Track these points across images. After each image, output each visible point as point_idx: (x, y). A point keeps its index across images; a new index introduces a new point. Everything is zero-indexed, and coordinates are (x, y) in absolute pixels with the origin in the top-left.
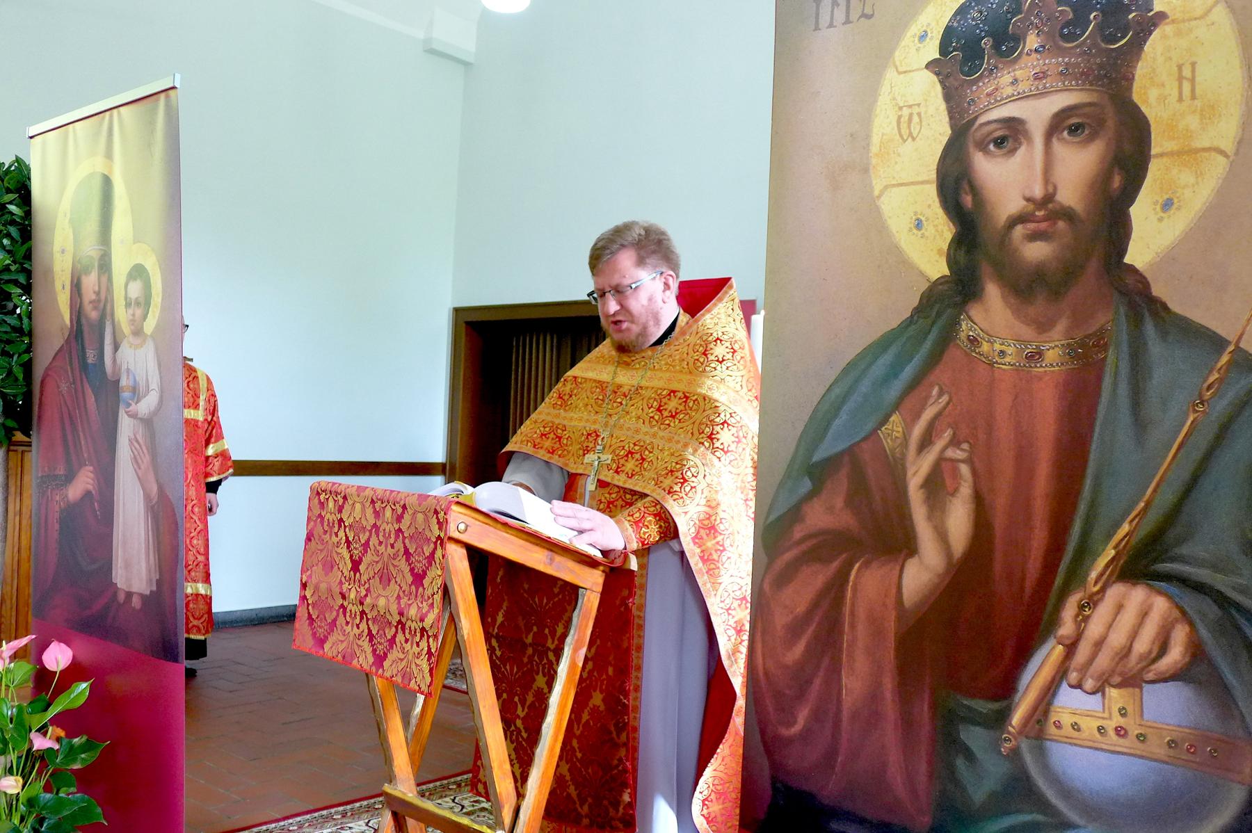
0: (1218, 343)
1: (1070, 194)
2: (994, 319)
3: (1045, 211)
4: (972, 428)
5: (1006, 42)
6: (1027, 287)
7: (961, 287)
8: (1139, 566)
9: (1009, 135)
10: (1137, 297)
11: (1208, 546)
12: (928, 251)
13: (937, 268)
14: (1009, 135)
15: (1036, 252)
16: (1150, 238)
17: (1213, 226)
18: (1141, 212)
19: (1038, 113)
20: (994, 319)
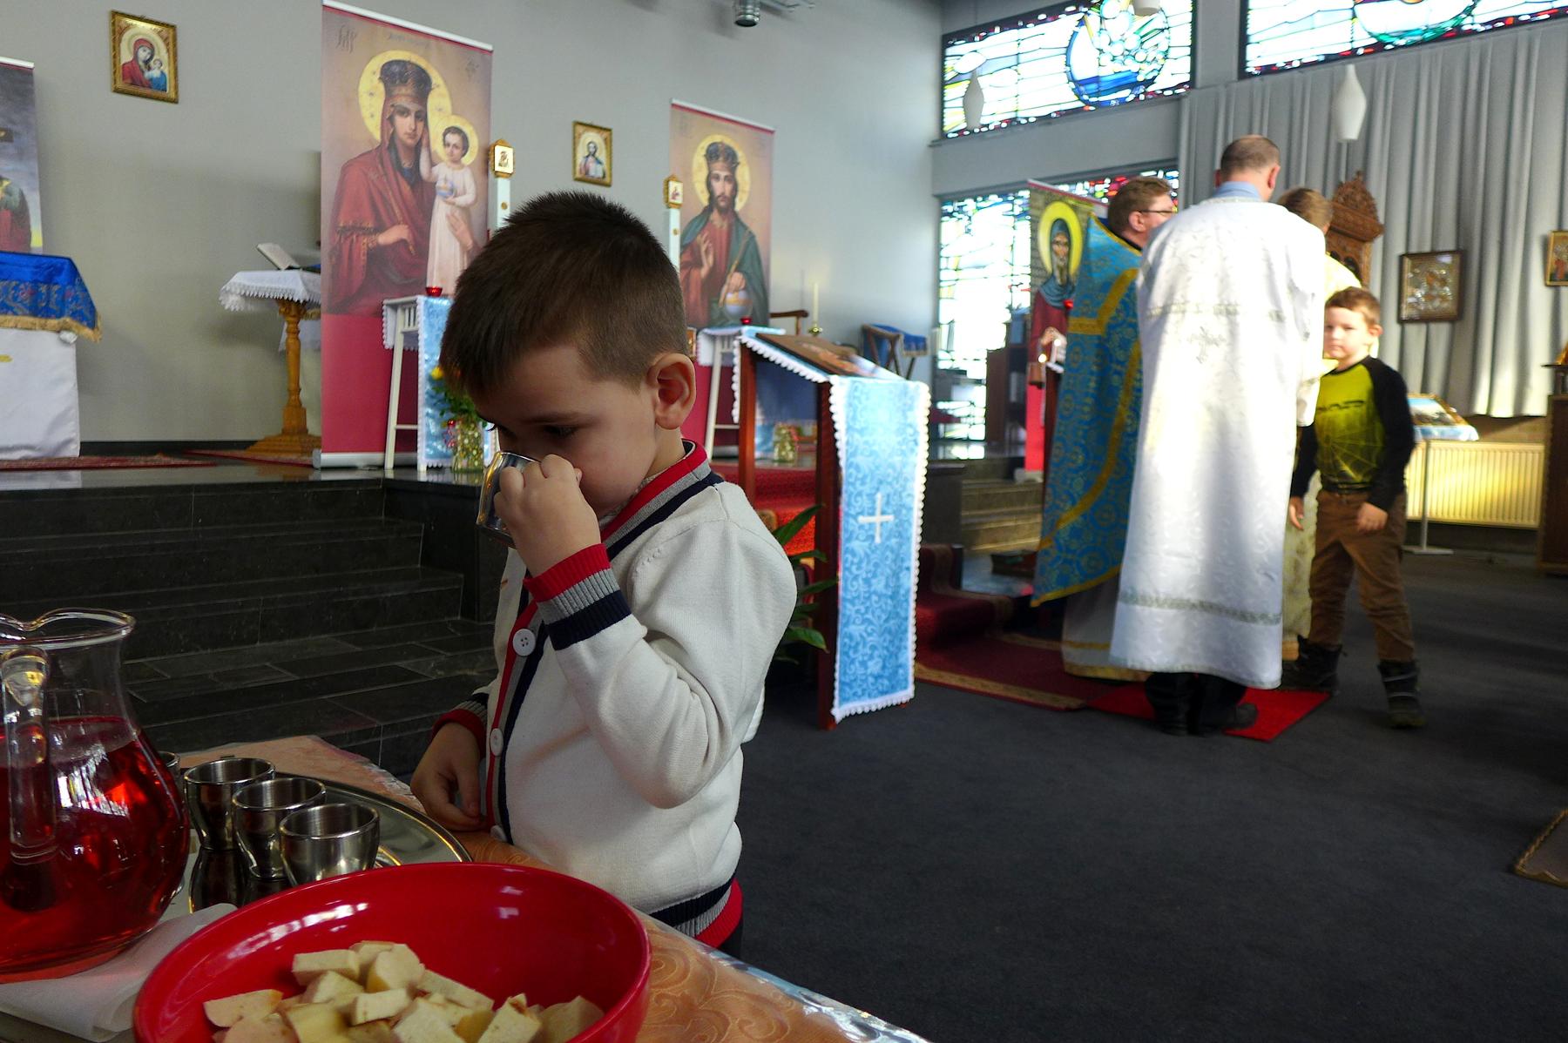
0: (745, 228)
1: (727, 193)
2: (715, 217)
3: (723, 194)
4: (712, 239)
5: (717, 157)
6: (722, 211)
7: (708, 210)
8: (737, 270)
9: (717, 178)
10: (735, 214)
11: (746, 266)
12: (704, 199)
13: (706, 203)
14: (717, 178)
15: (722, 204)
16: (739, 206)
17: (747, 206)
18: (737, 200)
19: (723, 174)
20: (715, 216)
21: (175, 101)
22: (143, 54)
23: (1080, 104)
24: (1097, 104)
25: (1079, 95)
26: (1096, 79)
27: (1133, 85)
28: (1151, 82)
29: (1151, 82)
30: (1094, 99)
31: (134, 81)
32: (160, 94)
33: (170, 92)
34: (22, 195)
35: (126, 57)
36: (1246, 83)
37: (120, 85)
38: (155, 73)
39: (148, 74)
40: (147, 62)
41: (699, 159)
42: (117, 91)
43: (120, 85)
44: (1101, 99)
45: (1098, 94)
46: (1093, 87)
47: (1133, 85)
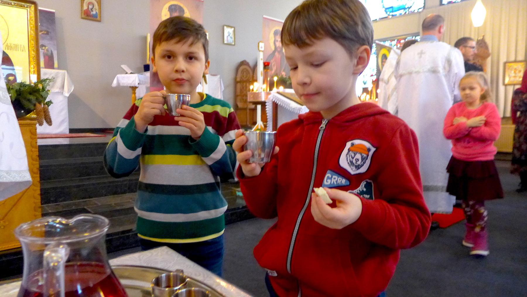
12: (273, 48)
14: (277, 41)
20: (277, 54)
21: (100, 21)
22: (90, 7)
23: (386, 15)
24: (392, 15)
25: (386, 12)
26: (392, 7)
27: (405, 9)
28: (409, 8)
29: (409, 8)
30: (391, 14)
31: (88, 15)
32: (95, 19)
33: (98, 18)
34: (51, 51)
35: (85, 8)
36: (442, 7)
37: (83, 16)
38: (94, 13)
39: (92, 13)
40: (92, 9)
41: (272, 35)
42: (82, 18)
43: (83, 16)
44: (394, 13)
45: (392, 12)
46: (391, 10)
47: (405, 9)
